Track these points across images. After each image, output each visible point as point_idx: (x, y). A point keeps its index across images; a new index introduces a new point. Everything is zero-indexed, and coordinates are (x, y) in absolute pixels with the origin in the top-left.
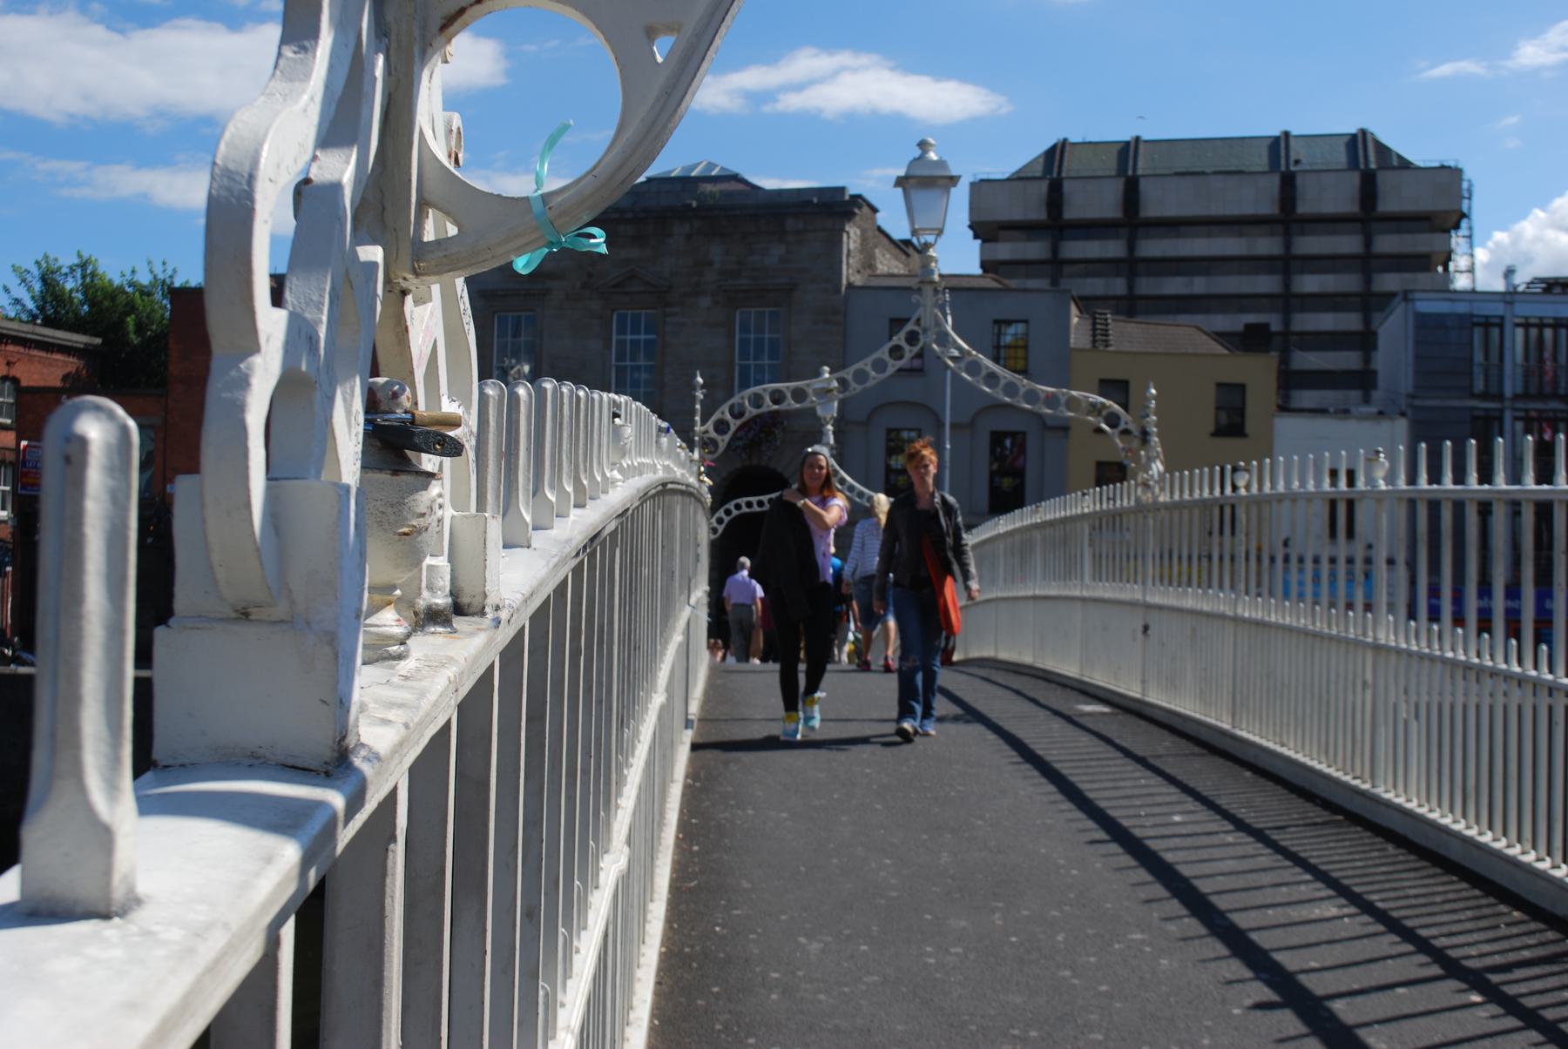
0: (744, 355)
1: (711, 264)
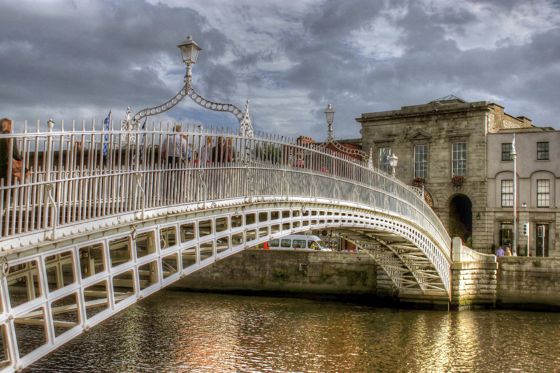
0: (455, 158)
1: (443, 129)
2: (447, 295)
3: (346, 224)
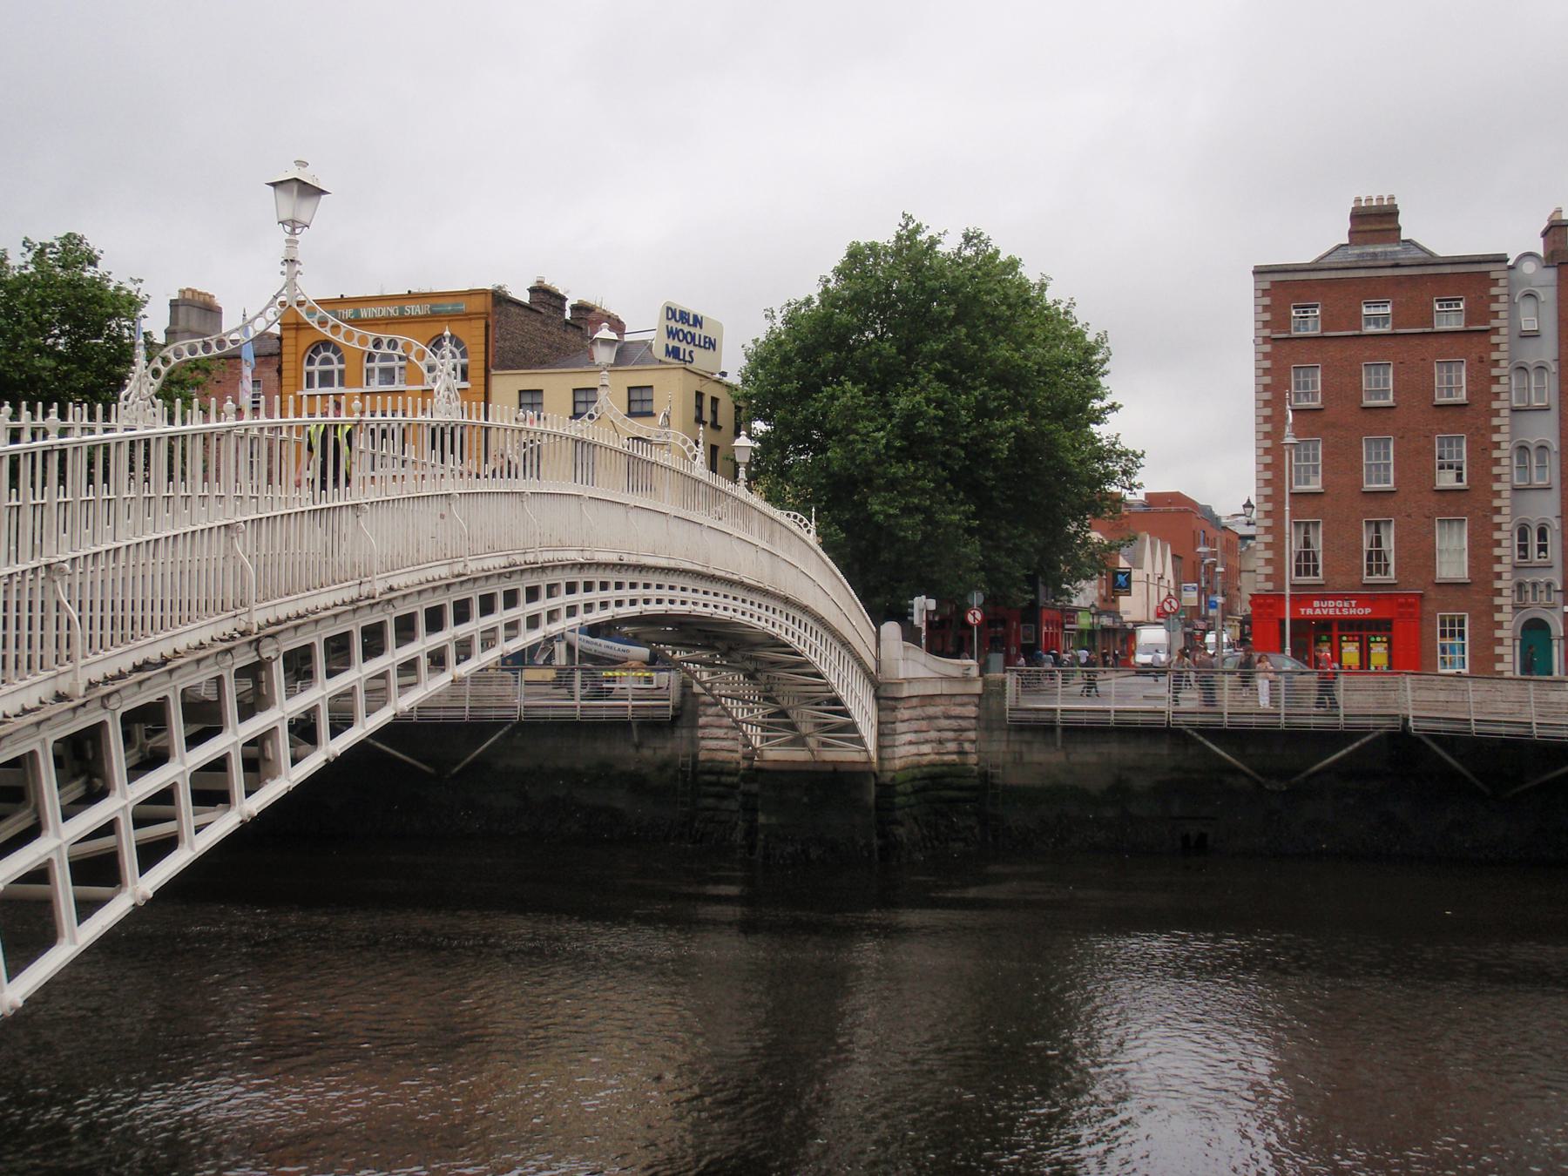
2: (869, 762)
3: (653, 608)
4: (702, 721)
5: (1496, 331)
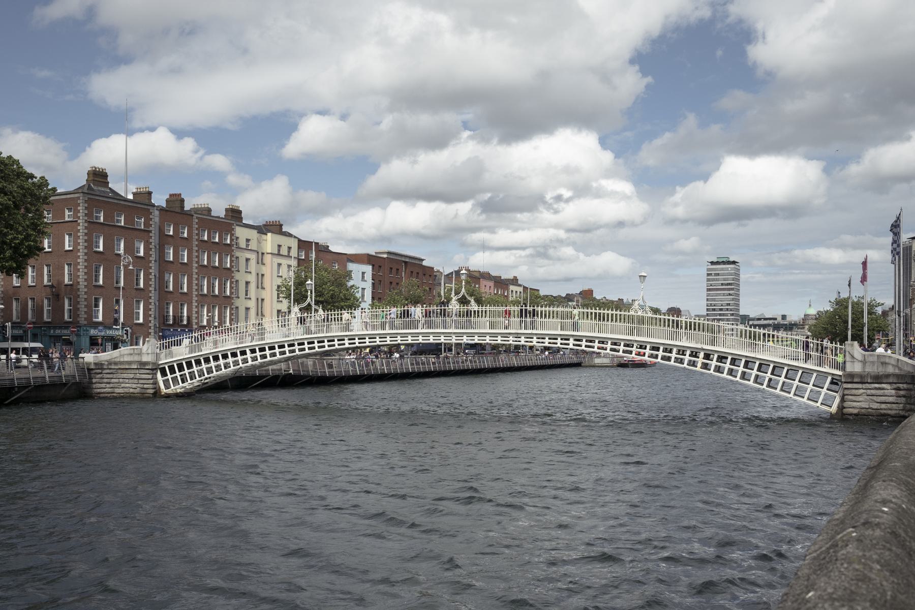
4: (94, 381)
5: (150, 231)
